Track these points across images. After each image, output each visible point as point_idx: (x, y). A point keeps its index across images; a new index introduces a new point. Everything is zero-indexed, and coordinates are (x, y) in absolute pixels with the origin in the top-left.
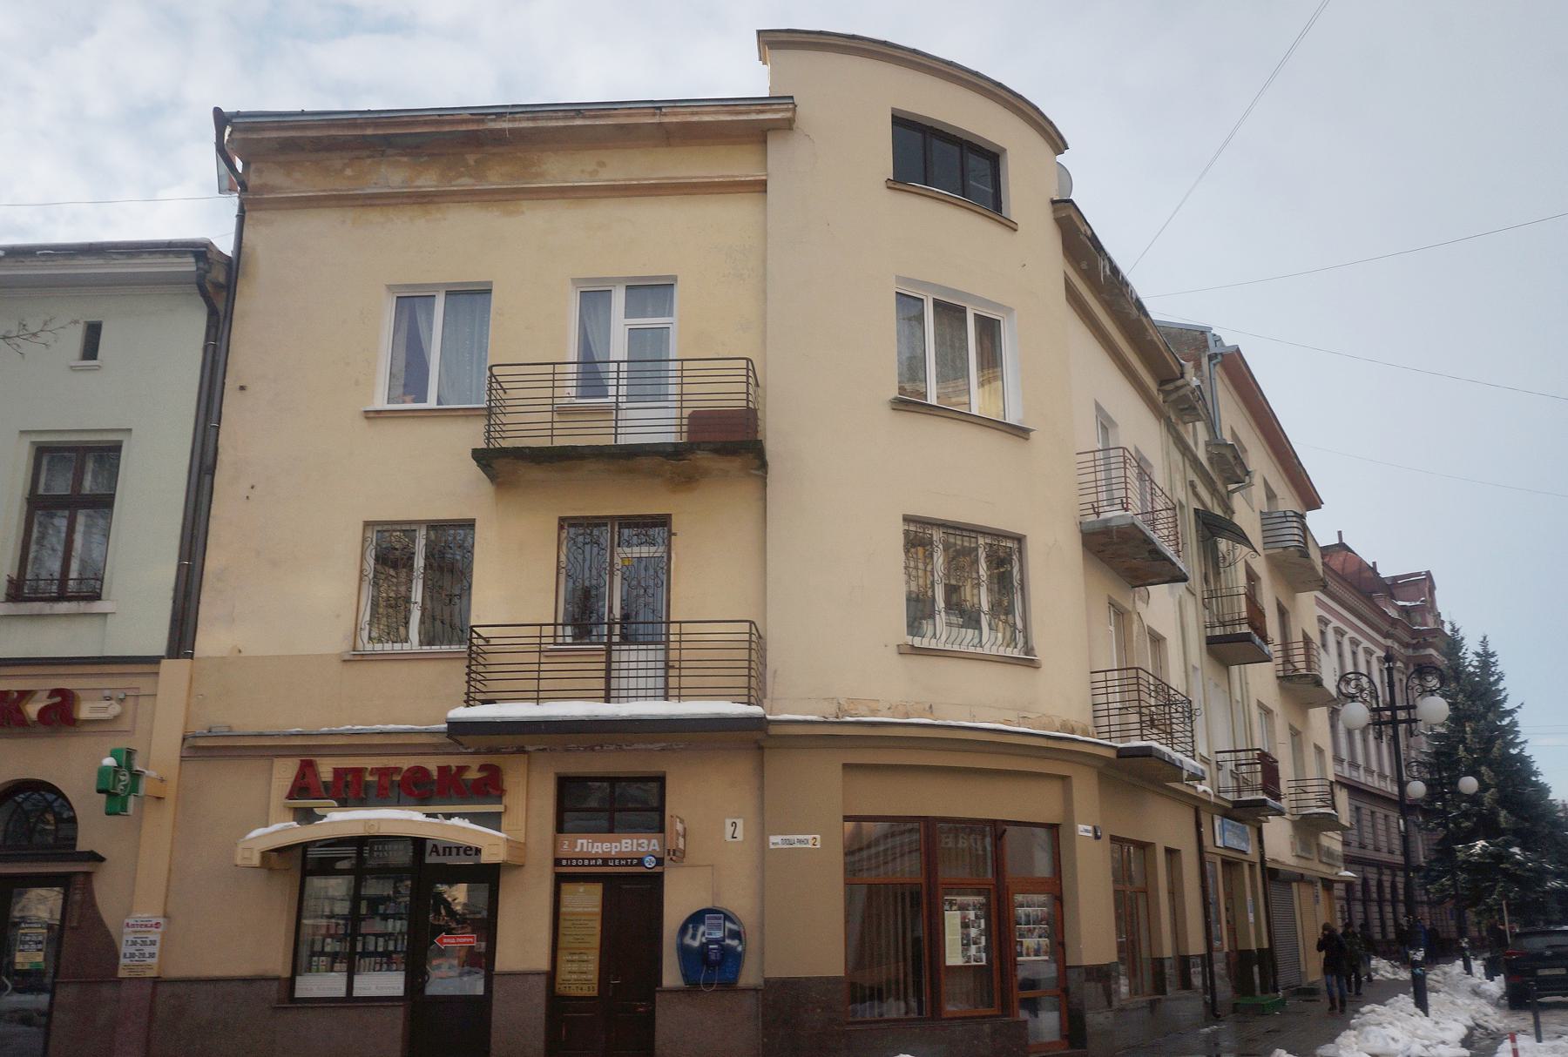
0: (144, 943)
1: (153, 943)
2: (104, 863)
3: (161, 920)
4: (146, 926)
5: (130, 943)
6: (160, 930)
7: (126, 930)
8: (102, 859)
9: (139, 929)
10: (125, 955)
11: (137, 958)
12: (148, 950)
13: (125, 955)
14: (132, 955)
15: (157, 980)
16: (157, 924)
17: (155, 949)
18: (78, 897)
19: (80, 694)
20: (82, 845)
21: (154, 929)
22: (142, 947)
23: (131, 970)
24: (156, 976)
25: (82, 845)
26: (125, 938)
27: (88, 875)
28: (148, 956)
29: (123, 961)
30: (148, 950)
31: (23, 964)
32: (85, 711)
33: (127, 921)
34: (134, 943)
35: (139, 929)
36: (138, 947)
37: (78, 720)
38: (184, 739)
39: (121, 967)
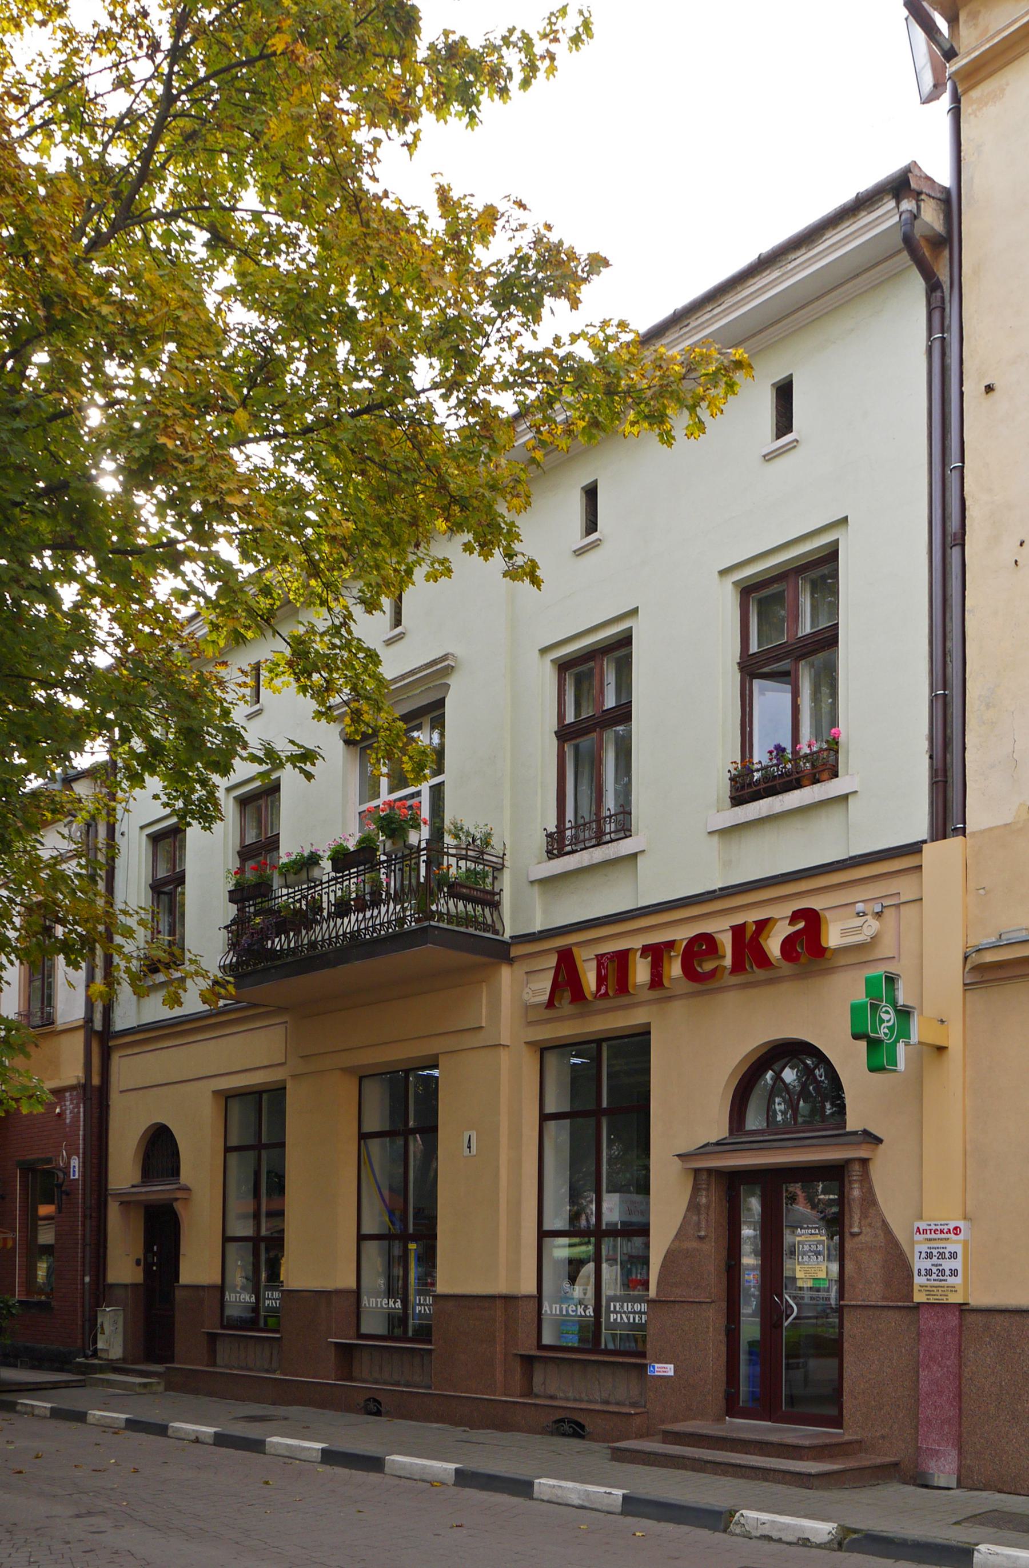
0: (942, 1256)
1: (954, 1255)
2: (881, 1147)
3: (961, 1224)
4: (942, 1232)
5: (923, 1255)
6: (961, 1237)
7: (918, 1237)
8: (879, 1141)
9: (933, 1236)
11: (934, 1276)
12: (948, 1265)
14: (929, 1272)
15: (964, 1307)
16: (956, 1228)
17: (957, 1264)
18: (856, 1193)
19: (828, 915)
21: (952, 1236)
22: (940, 1261)
23: (929, 1293)
24: (961, 1302)
25: (853, 1122)
26: (918, 1248)
27: (865, 1162)
28: (948, 1272)
29: (918, 1280)
30: (948, 1265)
33: (917, 1224)
34: (929, 1256)
35: (933, 1236)
36: (935, 1260)
37: (825, 949)
38: (966, 958)
39: (916, 1288)
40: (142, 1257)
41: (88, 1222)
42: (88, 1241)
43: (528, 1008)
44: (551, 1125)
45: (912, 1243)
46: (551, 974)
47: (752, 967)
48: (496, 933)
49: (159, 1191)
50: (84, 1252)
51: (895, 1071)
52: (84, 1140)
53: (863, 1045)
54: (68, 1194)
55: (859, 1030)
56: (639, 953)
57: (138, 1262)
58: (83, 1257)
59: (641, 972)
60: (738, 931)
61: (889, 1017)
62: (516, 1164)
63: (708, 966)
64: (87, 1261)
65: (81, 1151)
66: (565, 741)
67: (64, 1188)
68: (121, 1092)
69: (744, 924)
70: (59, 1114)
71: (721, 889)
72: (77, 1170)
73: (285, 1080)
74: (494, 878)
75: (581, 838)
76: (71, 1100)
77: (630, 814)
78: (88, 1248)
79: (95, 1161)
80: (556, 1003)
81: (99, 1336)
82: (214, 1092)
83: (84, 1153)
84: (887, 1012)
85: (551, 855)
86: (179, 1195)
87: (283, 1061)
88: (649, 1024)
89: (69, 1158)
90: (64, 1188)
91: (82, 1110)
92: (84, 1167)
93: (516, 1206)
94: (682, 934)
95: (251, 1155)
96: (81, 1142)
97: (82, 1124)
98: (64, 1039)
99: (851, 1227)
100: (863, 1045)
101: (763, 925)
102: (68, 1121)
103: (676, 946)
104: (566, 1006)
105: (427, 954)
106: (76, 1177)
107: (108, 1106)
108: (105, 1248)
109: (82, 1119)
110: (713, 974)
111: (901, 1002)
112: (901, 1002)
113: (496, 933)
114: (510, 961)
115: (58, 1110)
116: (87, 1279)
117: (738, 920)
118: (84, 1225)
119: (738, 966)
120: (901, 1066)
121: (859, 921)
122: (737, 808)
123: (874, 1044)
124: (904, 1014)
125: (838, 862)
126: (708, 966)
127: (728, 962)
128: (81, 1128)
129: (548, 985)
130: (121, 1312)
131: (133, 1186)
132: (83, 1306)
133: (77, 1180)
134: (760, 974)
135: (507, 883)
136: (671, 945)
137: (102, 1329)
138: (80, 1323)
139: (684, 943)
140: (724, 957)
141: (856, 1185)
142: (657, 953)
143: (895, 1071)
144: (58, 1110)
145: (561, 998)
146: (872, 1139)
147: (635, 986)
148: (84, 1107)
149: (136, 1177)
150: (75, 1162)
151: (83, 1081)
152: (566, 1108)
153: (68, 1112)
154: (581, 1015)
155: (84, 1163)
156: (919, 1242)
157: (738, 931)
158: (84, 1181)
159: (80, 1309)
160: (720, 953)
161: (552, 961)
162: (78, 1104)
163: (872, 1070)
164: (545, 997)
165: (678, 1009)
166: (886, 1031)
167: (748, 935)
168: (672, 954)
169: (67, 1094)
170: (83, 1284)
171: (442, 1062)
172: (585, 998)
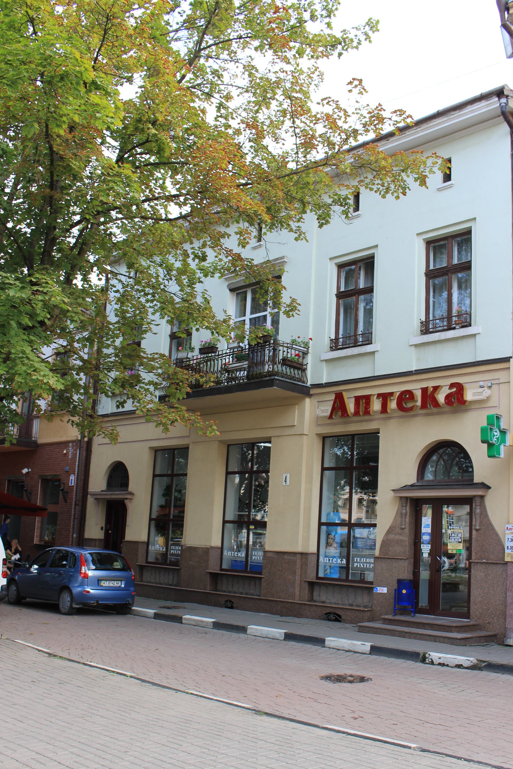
2: (490, 490)
5: (510, 540)
7: (507, 532)
8: (489, 488)
10: (508, 547)
13: (508, 547)
18: (478, 511)
19: (466, 386)
20: (477, 479)
25: (476, 480)
26: (507, 537)
27: (482, 497)
31: (452, 550)
32: (469, 396)
37: (466, 401)
40: (104, 526)
41: (77, 507)
42: (76, 517)
43: (318, 418)
44: (326, 472)
45: (504, 534)
46: (332, 403)
47: (430, 407)
48: (304, 382)
49: (117, 495)
51: (499, 457)
52: (78, 467)
53: (486, 445)
55: (484, 439)
56: (376, 396)
57: (102, 529)
59: (376, 405)
60: (424, 390)
61: (497, 434)
62: (309, 490)
63: (410, 405)
65: (76, 472)
66: (340, 299)
69: (427, 387)
71: (415, 371)
72: (73, 481)
73: (189, 444)
74: (304, 358)
75: (348, 343)
76: (73, 447)
77: (372, 334)
79: (82, 478)
80: (333, 417)
82: (150, 448)
83: (78, 473)
84: (496, 432)
85: (332, 349)
86: (128, 496)
87: (188, 435)
88: (379, 429)
91: (78, 452)
92: (77, 480)
93: (308, 509)
94: (397, 389)
95: (170, 478)
96: (77, 468)
97: (78, 459)
99: (475, 526)
100: (486, 445)
101: (436, 388)
102: (70, 457)
103: (394, 394)
104: (337, 419)
105: (275, 391)
106: (73, 485)
107: (91, 451)
108: (85, 520)
109: (78, 457)
110: (411, 409)
111: (502, 428)
112: (502, 428)
113: (304, 382)
114: (310, 396)
115: (65, 452)
117: (424, 385)
118: (75, 509)
119: (424, 406)
120: (502, 456)
121: (481, 390)
122: (424, 336)
123: (490, 445)
124: (503, 432)
125: (471, 363)
126: (410, 405)
127: (419, 403)
128: (77, 461)
129: (330, 409)
131: (102, 491)
133: (73, 486)
134: (435, 410)
135: (309, 360)
136: (391, 394)
139: (398, 394)
140: (417, 401)
141: (478, 507)
142: (385, 398)
143: (499, 457)
144: (65, 452)
145: (336, 414)
146: (486, 487)
147: (373, 412)
149: (104, 487)
150: (72, 478)
152: (332, 465)
153: (70, 453)
154: (346, 423)
155: (77, 478)
156: (508, 534)
157: (424, 390)
158: (77, 487)
160: (415, 399)
161: (333, 397)
162: (76, 450)
163: (489, 457)
164: (328, 414)
165: (393, 424)
166: (496, 440)
167: (429, 392)
168: (392, 398)
169: (71, 444)
170: (73, 538)
171: (273, 440)
172: (348, 415)
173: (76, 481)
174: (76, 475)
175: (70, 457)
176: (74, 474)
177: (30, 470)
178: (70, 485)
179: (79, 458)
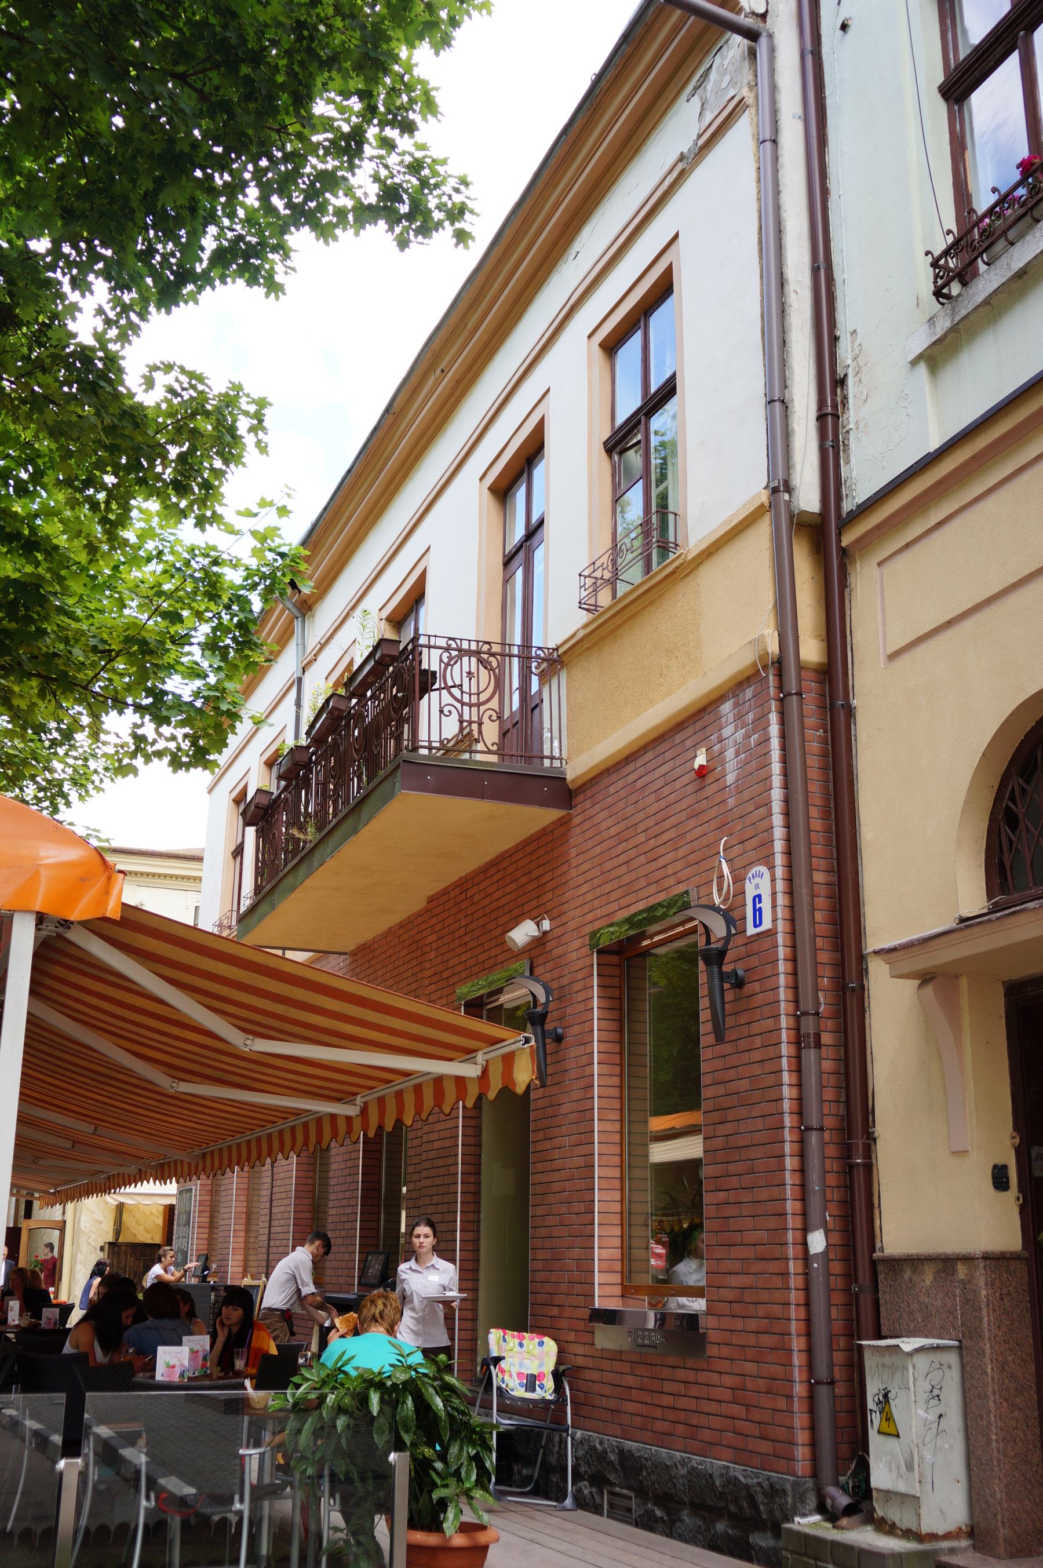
41: (810, 1055)
50: (802, 1155)
52: (787, 814)
54: (739, 983)
57: (999, 1179)
58: (802, 1171)
64: (815, 1184)
65: (779, 846)
67: (727, 968)
68: (893, 657)
70: (702, 773)
76: (739, 717)
78: (814, 1138)
81: (875, 1440)
89: (739, 879)
90: (727, 968)
91: (774, 730)
92: (790, 893)
96: (778, 820)
97: (776, 768)
98: (709, 576)
102: (730, 779)
106: (767, 924)
107: (850, 712)
109: (776, 754)
115: (701, 760)
116: (817, 1242)
118: (798, 1069)
128: (777, 780)
130: (953, 1359)
131: (962, 920)
132: (809, 1334)
133: (771, 933)
137: (889, 1418)
138: (799, 1389)
148: (782, 722)
151: (773, 647)
153: (730, 753)
155: (790, 880)
159: (797, 1344)
169: (727, 707)
173: (781, 899)
174: (779, 859)
175: (730, 779)
176: (768, 861)
177: (546, 925)
178: (751, 930)
179: (784, 760)
